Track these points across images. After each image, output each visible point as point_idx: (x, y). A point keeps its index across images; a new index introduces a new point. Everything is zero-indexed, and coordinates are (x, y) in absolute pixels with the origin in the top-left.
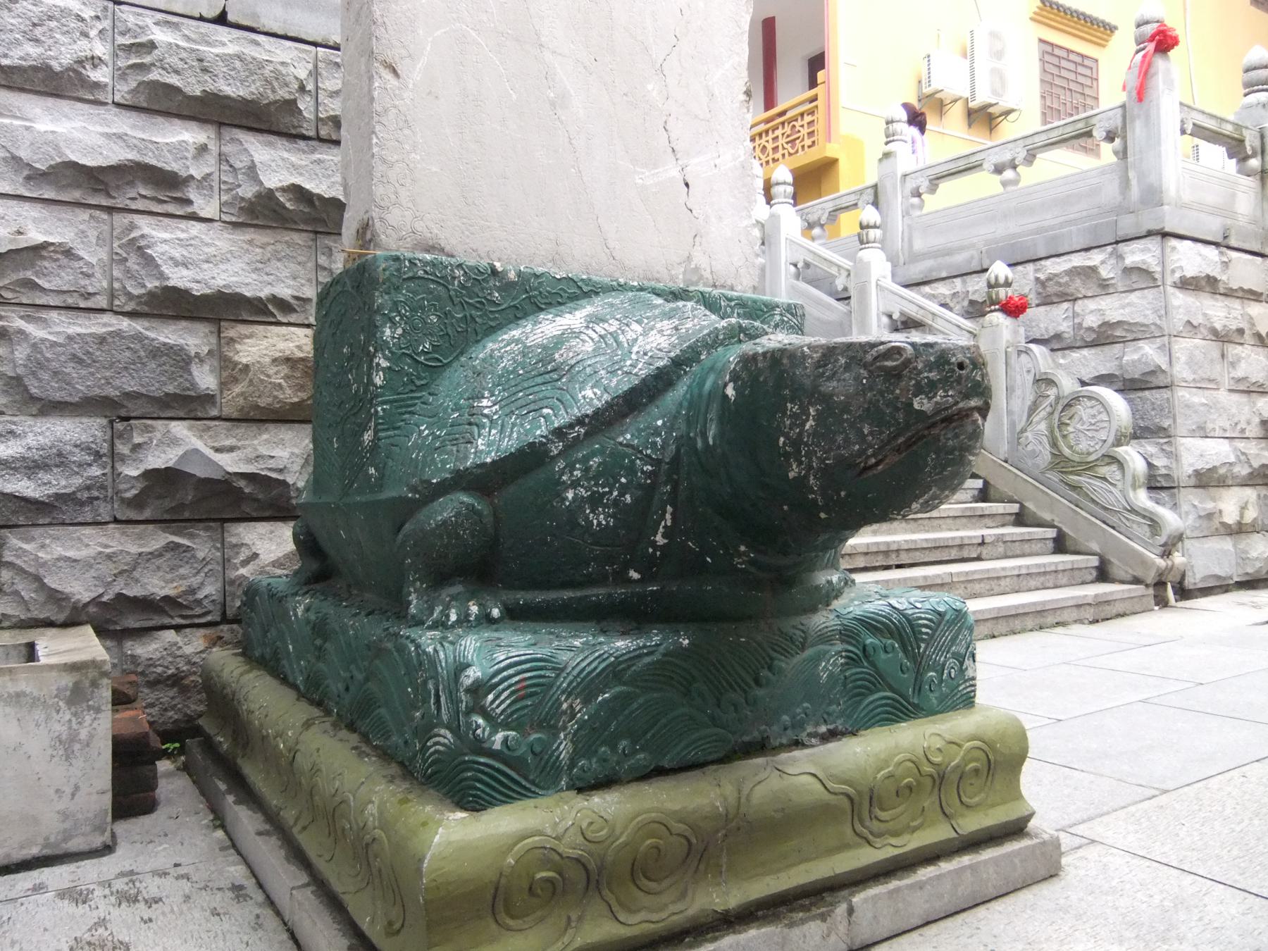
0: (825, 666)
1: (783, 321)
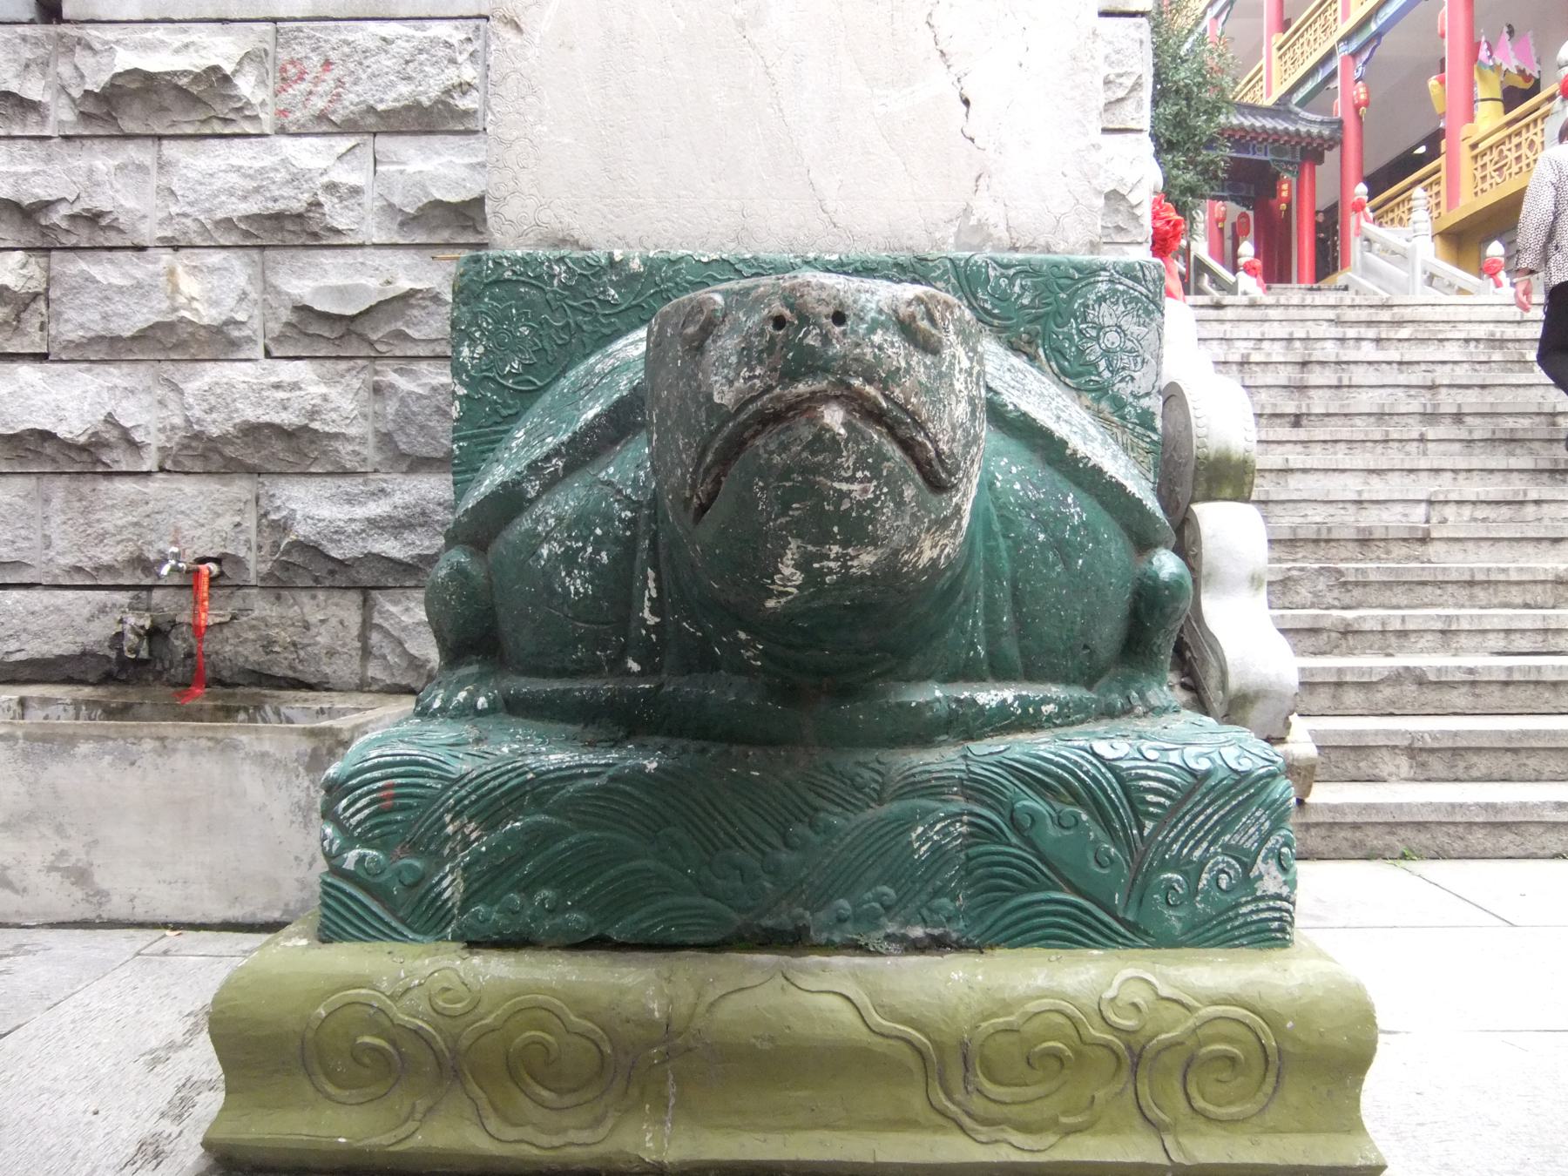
0: (924, 832)
1: (1116, 291)
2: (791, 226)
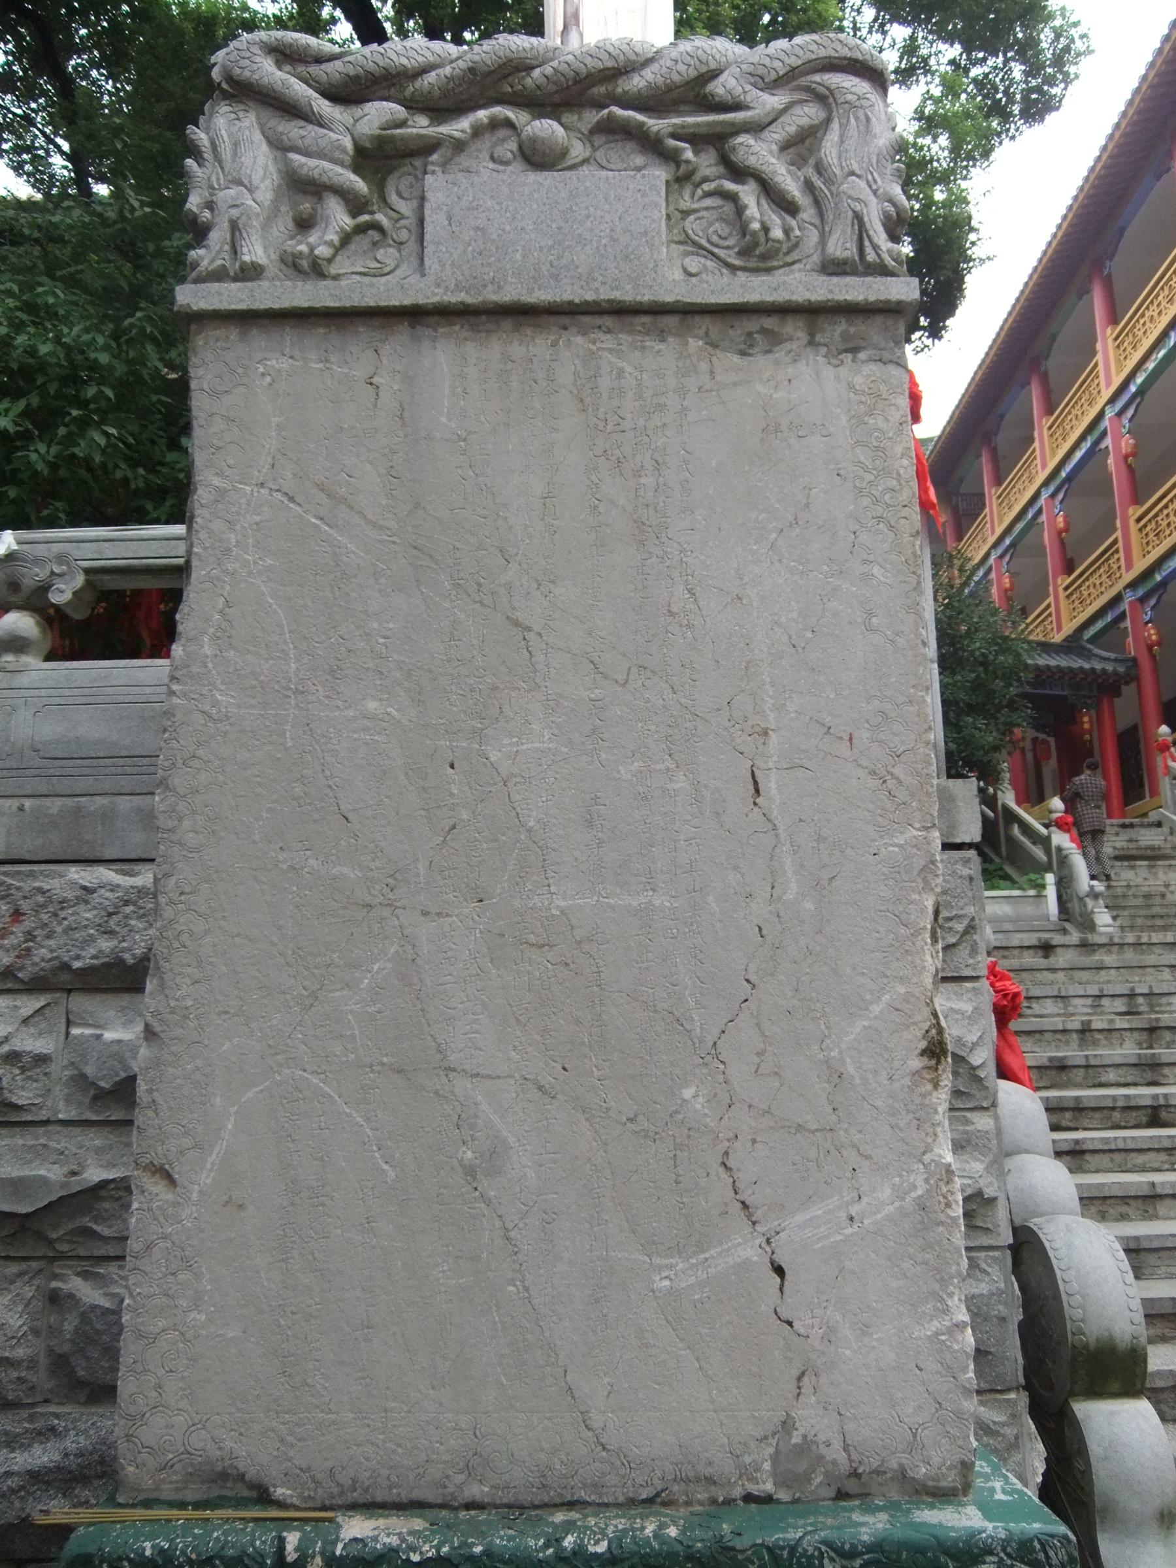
2: (542, 1450)
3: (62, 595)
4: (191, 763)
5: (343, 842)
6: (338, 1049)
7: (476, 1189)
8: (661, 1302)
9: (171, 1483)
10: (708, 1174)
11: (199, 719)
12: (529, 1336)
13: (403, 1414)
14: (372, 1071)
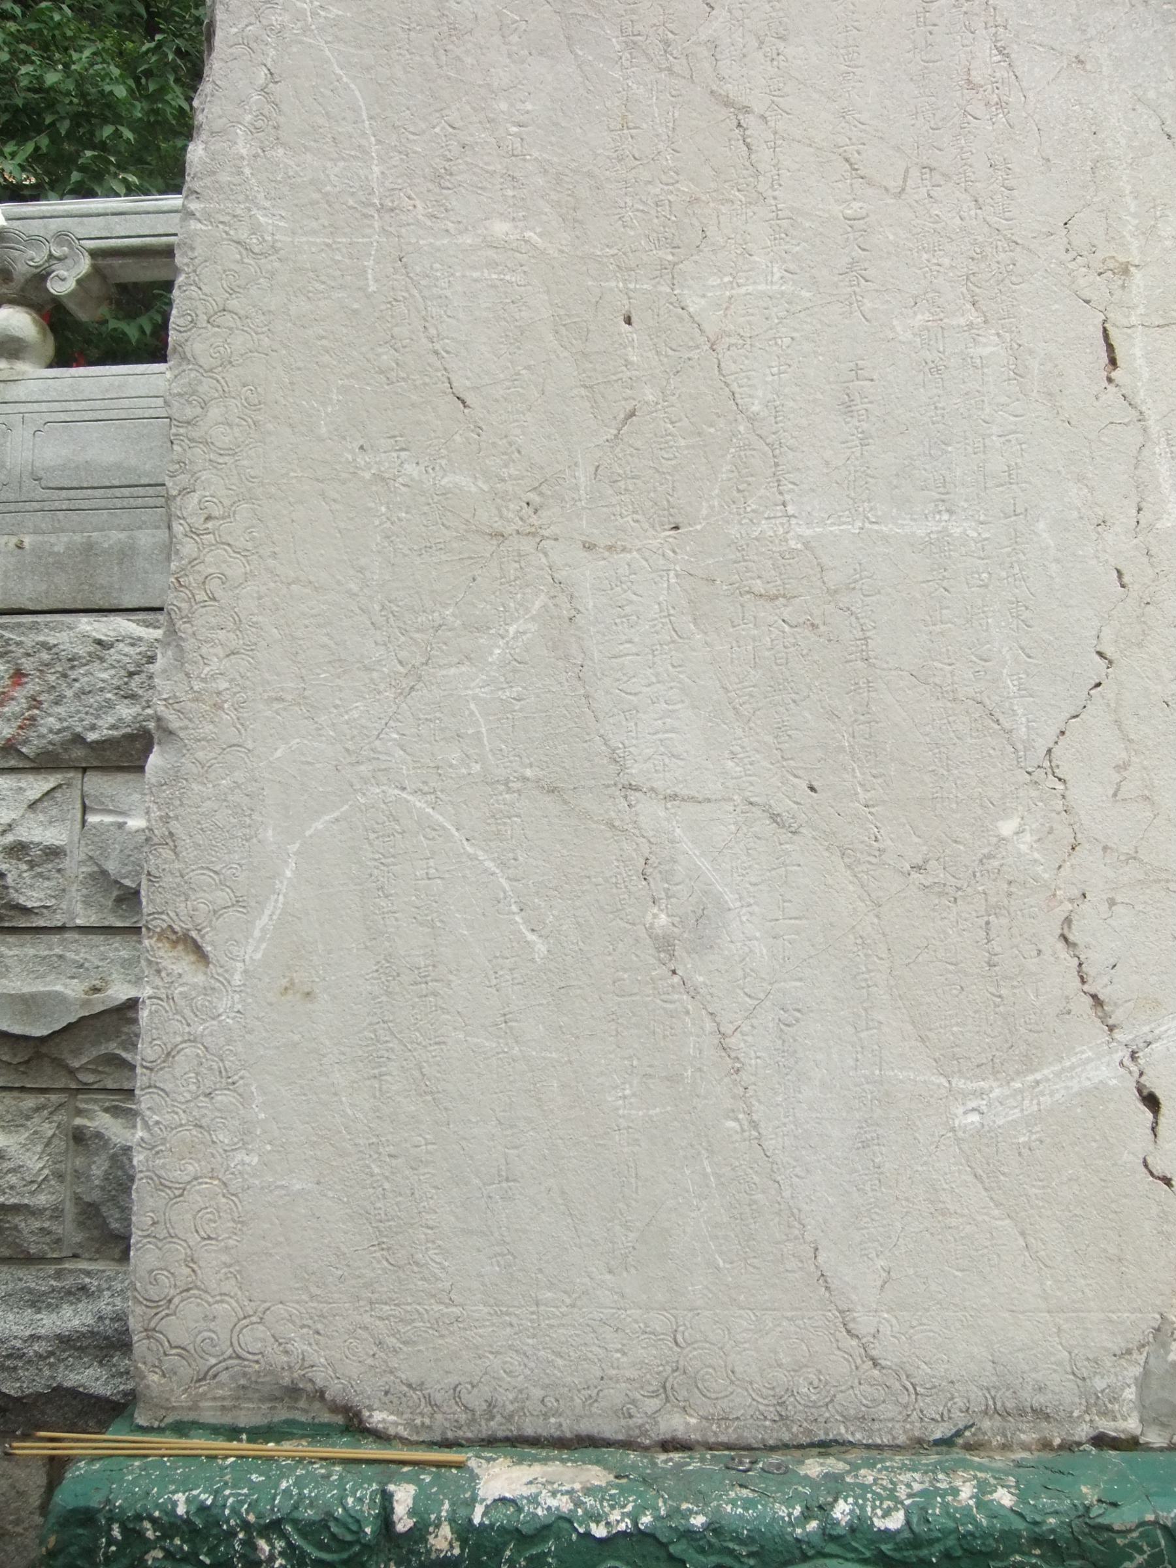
2: (779, 1366)
3: (62, 284)
4: (219, 321)
5: (457, 438)
6: (455, 756)
7: (674, 972)
8: (965, 1146)
9: (215, 1399)
10: (1039, 952)
11: (234, 252)
12: (759, 1196)
13: (564, 1309)
14: (509, 790)
